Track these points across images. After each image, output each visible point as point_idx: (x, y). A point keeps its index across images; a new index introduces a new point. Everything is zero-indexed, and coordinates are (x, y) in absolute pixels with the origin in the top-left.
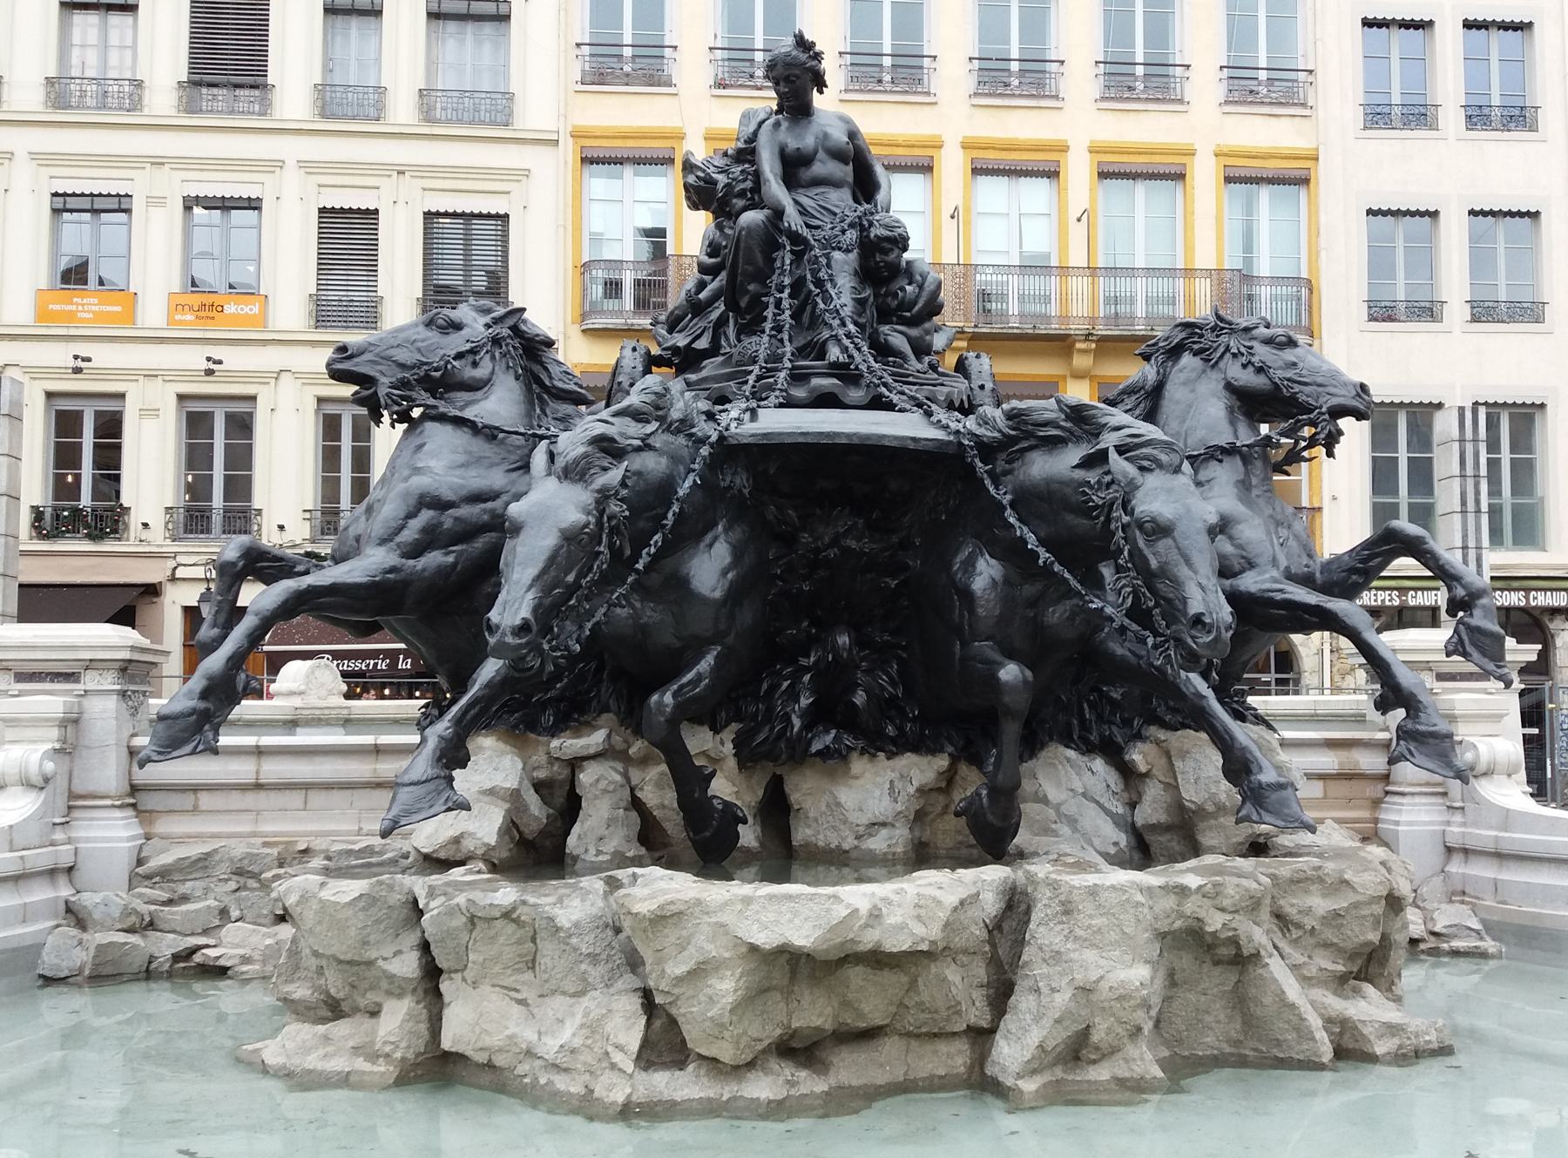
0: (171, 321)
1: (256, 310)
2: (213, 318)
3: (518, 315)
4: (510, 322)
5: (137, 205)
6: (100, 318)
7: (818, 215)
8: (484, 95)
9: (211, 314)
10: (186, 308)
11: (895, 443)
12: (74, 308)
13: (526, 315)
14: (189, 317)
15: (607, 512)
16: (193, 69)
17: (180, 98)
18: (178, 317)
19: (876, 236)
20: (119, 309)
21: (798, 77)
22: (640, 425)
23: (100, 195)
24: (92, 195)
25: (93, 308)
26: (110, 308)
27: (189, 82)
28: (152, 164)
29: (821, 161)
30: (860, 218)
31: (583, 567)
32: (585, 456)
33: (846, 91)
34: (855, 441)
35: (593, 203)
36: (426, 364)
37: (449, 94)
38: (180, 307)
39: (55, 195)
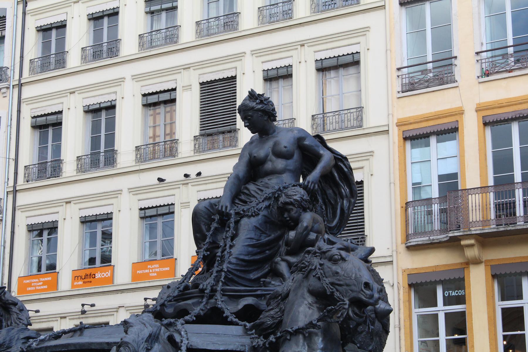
5: (177, 209)
8: (346, 112)
9: (90, 280)
11: (98, 347)
12: (147, 271)
16: (202, 128)
17: (195, 145)
19: (281, 203)
20: (167, 269)
21: (251, 116)
23: (160, 206)
24: (156, 207)
25: (157, 270)
26: (164, 269)
27: (201, 135)
28: (183, 184)
29: (271, 161)
34: (78, 348)
35: (414, 165)
37: (352, 111)
38: (76, 278)
39: (141, 209)
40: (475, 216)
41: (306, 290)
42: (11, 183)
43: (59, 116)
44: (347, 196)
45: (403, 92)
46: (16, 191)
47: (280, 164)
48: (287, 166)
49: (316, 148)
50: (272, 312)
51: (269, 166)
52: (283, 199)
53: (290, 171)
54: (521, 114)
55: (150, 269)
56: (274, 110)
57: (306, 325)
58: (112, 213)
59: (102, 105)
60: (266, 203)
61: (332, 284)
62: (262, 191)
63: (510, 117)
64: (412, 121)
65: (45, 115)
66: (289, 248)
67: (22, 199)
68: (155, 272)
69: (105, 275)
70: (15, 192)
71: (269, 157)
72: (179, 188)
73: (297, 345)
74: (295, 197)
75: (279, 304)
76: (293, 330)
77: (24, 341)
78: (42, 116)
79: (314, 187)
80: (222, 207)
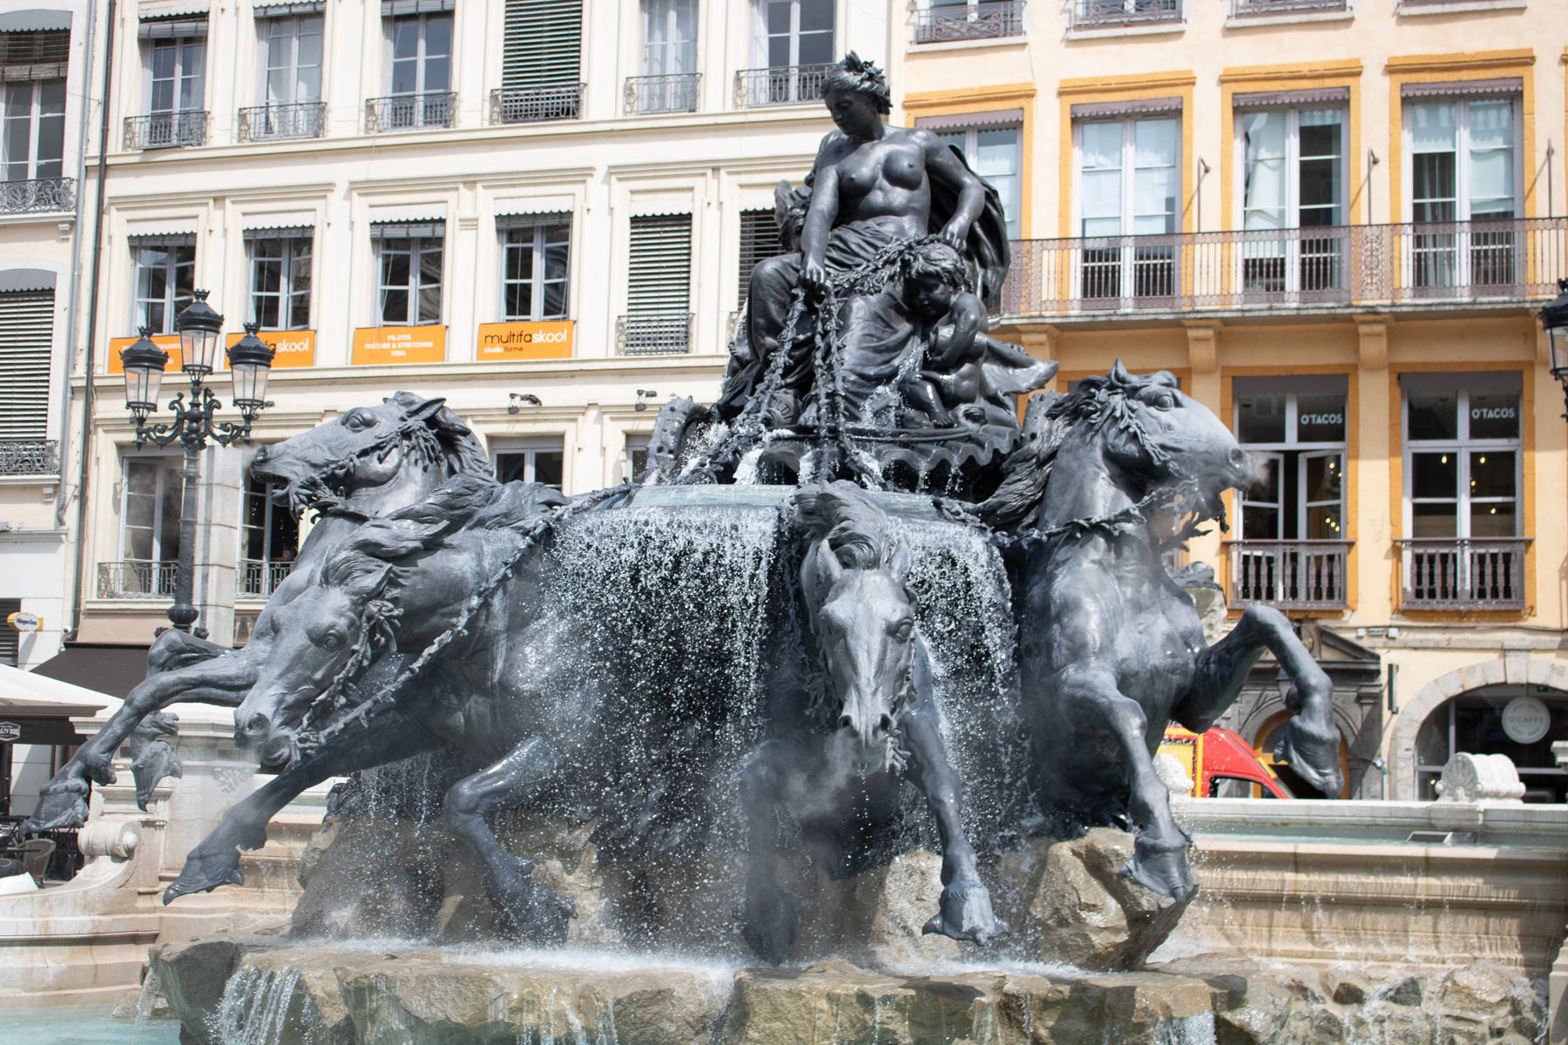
0: (481, 355)
1: (564, 337)
2: (521, 349)
3: (437, 406)
4: (427, 413)
6: (413, 354)
7: (862, 253)
10: (496, 339)
12: (385, 346)
13: (445, 404)
14: (499, 349)
15: (366, 612)
18: (487, 350)
19: (917, 272)
20: (430, 344)
21: (850, 103)
22: (423, 526)
23: (416, 222)
25: (408, 345)
29: (881, 189)
30: (901, 252)
31: (334, 665)
32: (347, 560)
33: (1238, 16)
36: (333, 462)
39: (375, 223)
40: (1049, 292)
41: (1098, 454)
42: (94, 149)
43: (201, 25)
44: (994, 263)
45: (919, 43)
46: (107, 166)
47: (899, 196)
48: (910, 201)
49: (955, 170)
50: (1020, 486)
51: (877, 198)
52: (919, 265)
53: (915, 211)
54: (1144, 106)
55: (391, 342)
56: (888, 93)
57: (1116, 516)
58: (312, 227)
59: (294, 10)
60: (886, 273)
61: (1163, 447)
62: (876, 248)
63: (1123, 111)
64: (935, 100)
65: (170, 18)
66: (939, 358)
67: (116, 186)
68: (402, 349)
69: (297, 347)
70: (103, 170)
71: (878, 183)
72: (457, 189)
73: (1096, 548)
74: (944, 264)
75: (1033, 471)
76: (1091, 524)
77: (544, 507)
78: (162, 19)
79: (961, 244)
80: (811, 273)
